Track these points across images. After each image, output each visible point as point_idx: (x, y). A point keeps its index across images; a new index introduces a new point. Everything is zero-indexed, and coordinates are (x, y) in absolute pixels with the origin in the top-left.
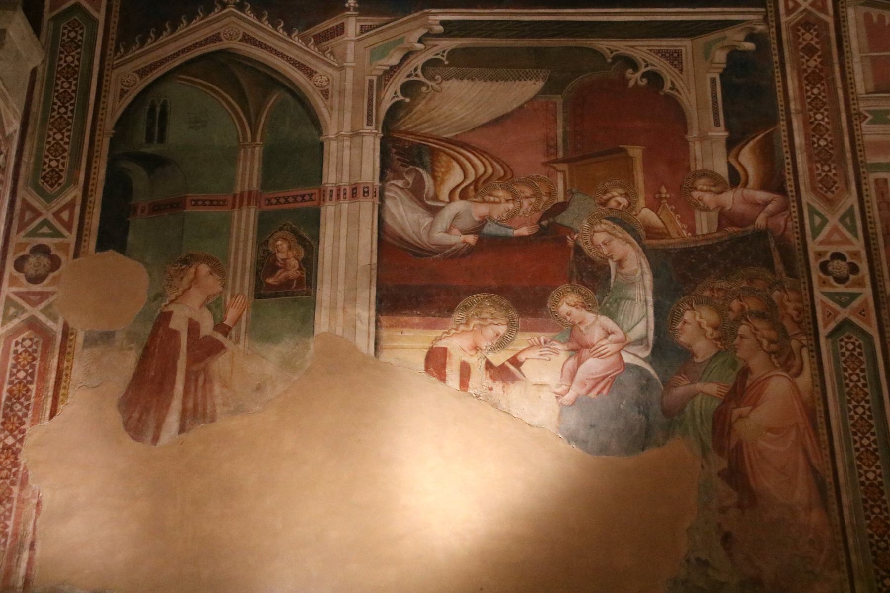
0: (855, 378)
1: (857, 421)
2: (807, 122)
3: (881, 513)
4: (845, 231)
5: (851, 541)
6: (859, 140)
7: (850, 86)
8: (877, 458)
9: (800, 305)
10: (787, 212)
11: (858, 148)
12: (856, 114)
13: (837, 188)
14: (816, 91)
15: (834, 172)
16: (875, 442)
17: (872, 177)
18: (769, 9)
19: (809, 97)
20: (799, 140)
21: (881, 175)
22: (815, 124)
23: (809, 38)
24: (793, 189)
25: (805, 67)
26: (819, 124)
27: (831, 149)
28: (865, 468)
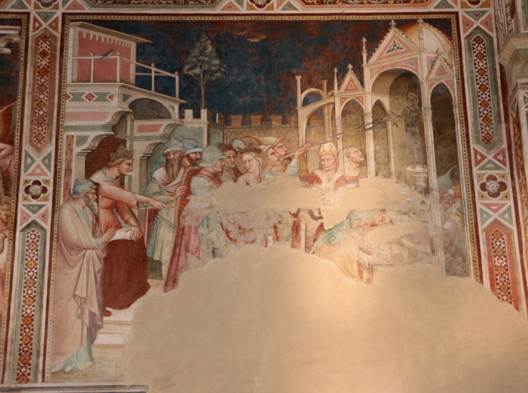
0: (32, 255)
1: (28, 280)
2: (34, 100)
3: (29, 332)
4: (44, 167)
5: (9, 348)
6: (63, 111)
7: (63, 77)
8: (34, 301)
9: (8, 213)
10: (12, 156)
11: (61, 116)
12: (64, 95)
13: (44, 141)
14: (43, 80)
15: (44, 131)
16: (35, 292)
17: (66, 134)
18: (23, 27)
19: (38, 84)
20: (27, 111)
21: (71, 133)
22: (38, 101)
23: (44, 46)
24: (18, 141)
25: (39, 65)
26: (41, 101)
27: (45, 116)
28: (26, 307)
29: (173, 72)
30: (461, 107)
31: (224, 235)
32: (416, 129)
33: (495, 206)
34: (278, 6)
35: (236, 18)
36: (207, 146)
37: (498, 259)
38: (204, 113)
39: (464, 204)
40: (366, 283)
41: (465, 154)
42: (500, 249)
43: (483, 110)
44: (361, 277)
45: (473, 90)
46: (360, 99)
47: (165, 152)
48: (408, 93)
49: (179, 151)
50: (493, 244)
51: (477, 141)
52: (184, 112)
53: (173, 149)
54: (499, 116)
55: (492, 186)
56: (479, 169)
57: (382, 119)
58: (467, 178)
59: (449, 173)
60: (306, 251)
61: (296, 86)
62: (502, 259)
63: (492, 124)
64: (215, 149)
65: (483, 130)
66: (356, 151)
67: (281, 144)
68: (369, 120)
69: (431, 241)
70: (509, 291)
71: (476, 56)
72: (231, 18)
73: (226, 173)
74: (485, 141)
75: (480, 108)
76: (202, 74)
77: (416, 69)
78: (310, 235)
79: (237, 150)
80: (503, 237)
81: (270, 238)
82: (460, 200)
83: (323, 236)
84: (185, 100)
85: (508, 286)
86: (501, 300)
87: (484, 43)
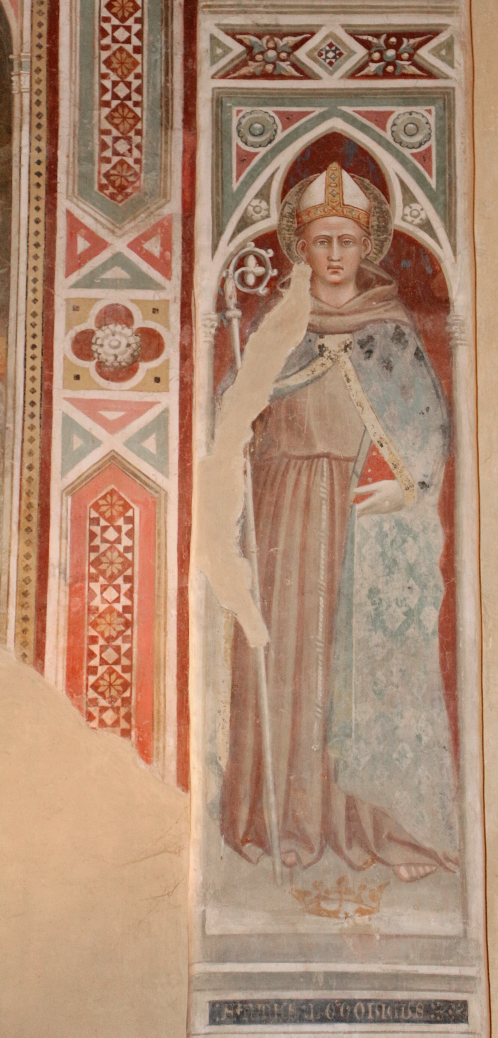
30: (38, 70)
33: (116, 410)
37: (104, 588)
39: (10, 401)
41: (37, 233)
42: (116, 554)
43: (115, 84)
50: (93, 535)
54: (167, 104)
55: (115, 343)
56: (76, 286)
58: (34, 315)
62: (118, 588)
63: (139, 133)
65: (108, 153)
70: (127, 694)
74: (111, 190)
75: (104, 76)
80: (130, 513)
85: (127, 676)
86: (95, 724)
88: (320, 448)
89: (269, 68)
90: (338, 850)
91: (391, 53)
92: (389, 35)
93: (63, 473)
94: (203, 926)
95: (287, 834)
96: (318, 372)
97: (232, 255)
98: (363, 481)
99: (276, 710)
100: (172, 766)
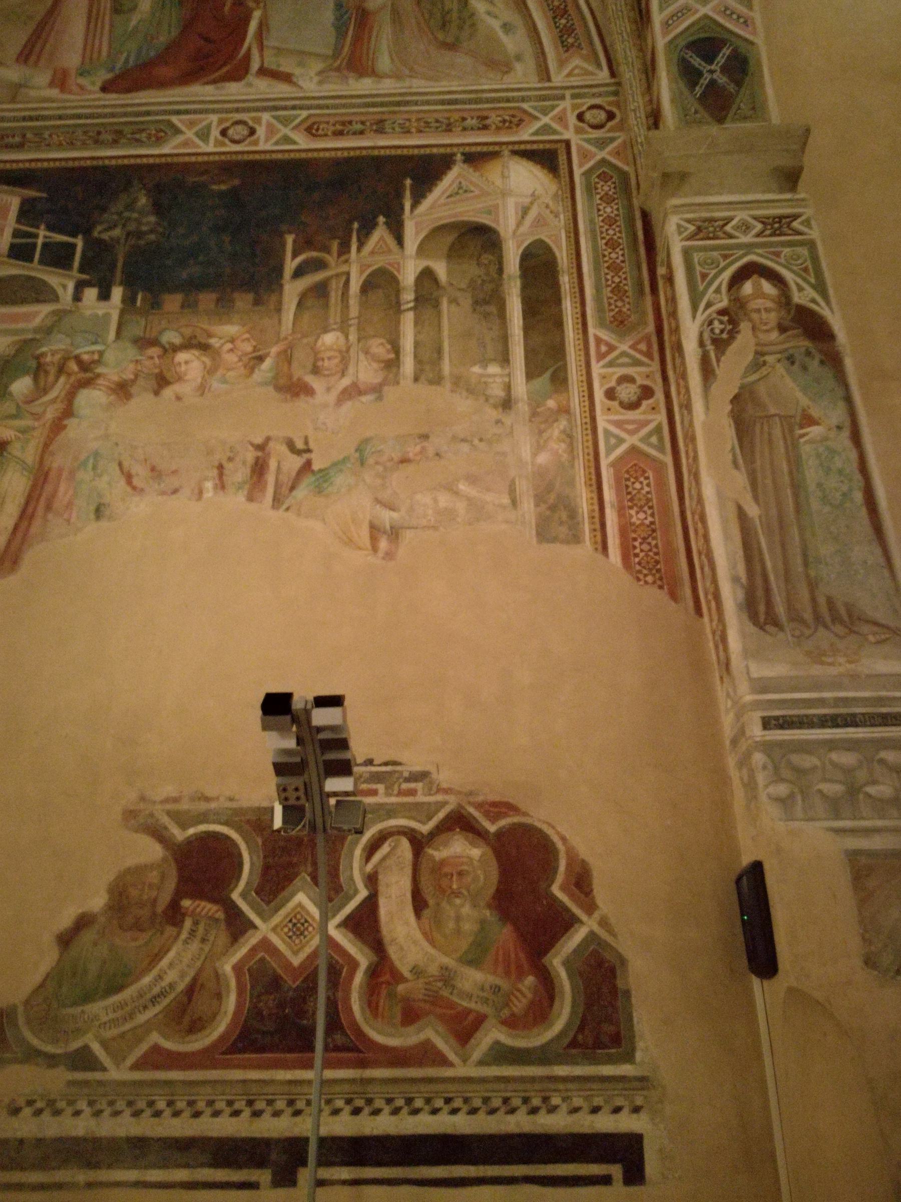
29: (74, 236)
31: (122, 482)
32: (493, 309)
34: (267, 140)
35: (193, 159)
36: (114, 342)
37: (637, 513)
38: (117, 293)
40: (383, 558)
44: (375, 549)
45: (595, 248)
46: (396, 266)
47: (38, 352)
48: (480, 255)
49: (63, 350)
50: (627, 487)
51: (602, 324)
52: (82, 292)
53: (53, 348)
56: (603, 367)
57: (431, 294)
59: (548, 375)
60: (274, 507)
61: (284, 251)
62: (645, 512)
63: (627, 297)
64: (128, 345)
66: (382, 344)
67: (247, 336)
68: (408, 297)
69: (510, 486)
70: (658, 567)
71: (601, 199)
72: (187, 159)
73: (141, 382)
76: (124, 237)
77: (498, 222)
78: (284, 478)
79: (167, 346)
80: (646, 475)
81: (209, 485)
82: (567, 417)
83: (308, 480)
84: (88, 274)
85: (657, 557)
86: (642, 583)
87: (614, 180)
88: (773, 411)
89: (711, 235)
90: (826, 627)
91: (777, 225)
92: (774, 218)
93: (608, 453)
94: (748, 673)
95: (792, 620)
96: (765, 373)
97: (705, 321)
98: (801, 427)
99: (771, 550)
100: (691, 604)
